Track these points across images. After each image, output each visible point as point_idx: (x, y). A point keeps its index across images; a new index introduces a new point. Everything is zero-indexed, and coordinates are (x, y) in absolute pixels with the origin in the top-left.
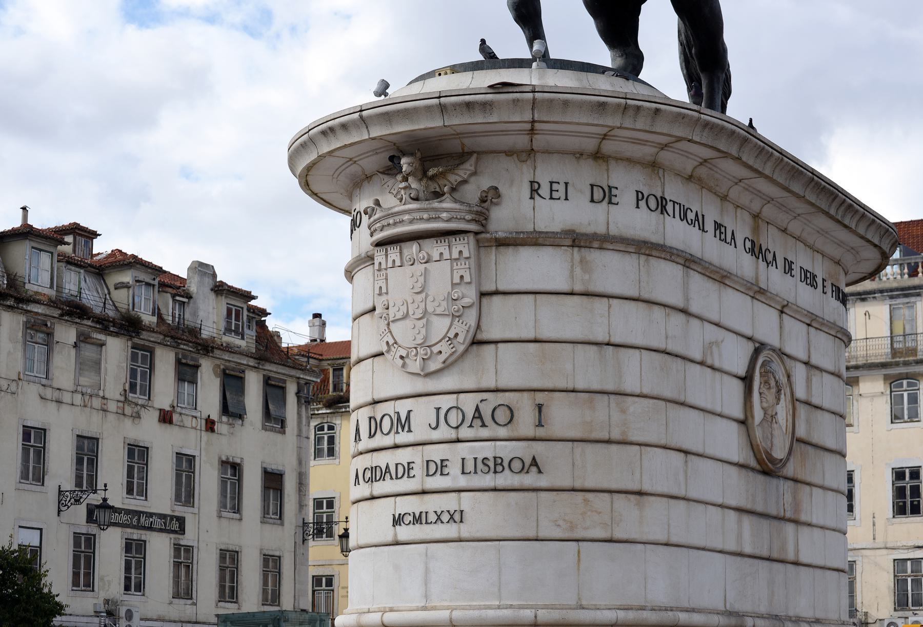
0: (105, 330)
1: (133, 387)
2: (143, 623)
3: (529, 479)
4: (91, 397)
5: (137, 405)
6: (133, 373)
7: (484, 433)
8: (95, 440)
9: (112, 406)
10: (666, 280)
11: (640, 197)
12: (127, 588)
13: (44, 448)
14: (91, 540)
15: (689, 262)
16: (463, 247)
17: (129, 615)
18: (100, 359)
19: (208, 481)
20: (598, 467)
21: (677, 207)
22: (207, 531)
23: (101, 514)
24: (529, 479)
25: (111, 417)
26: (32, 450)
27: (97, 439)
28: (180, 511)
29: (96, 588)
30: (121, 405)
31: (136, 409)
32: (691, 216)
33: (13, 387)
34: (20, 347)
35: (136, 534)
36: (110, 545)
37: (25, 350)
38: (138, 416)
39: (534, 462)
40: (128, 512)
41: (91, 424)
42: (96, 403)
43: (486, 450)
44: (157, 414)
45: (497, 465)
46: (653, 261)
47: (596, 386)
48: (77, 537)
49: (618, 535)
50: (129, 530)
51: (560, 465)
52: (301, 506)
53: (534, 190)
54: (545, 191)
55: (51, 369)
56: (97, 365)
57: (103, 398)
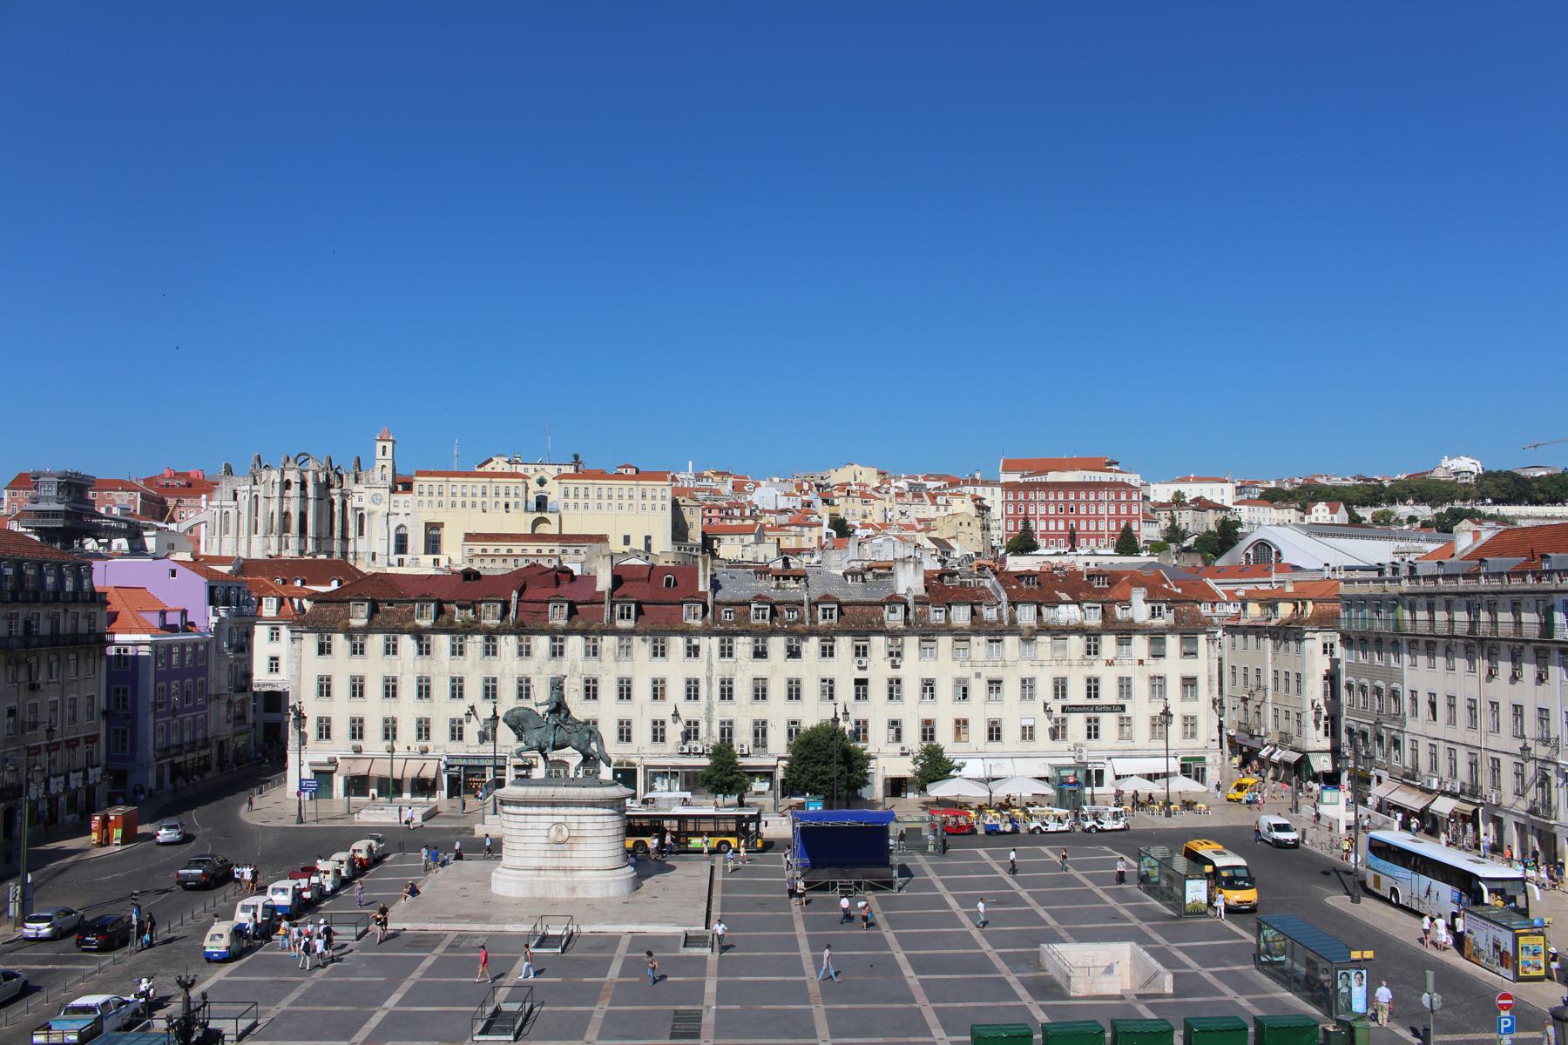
1: (1089, 653)
8: (1064, 680)
10: (521, 818)
12: (1089, 736)
19: (1141, 687)
22: (1142, 708)
28: (1121, 702)
36: (1077, 723)
52: (1210, 691)
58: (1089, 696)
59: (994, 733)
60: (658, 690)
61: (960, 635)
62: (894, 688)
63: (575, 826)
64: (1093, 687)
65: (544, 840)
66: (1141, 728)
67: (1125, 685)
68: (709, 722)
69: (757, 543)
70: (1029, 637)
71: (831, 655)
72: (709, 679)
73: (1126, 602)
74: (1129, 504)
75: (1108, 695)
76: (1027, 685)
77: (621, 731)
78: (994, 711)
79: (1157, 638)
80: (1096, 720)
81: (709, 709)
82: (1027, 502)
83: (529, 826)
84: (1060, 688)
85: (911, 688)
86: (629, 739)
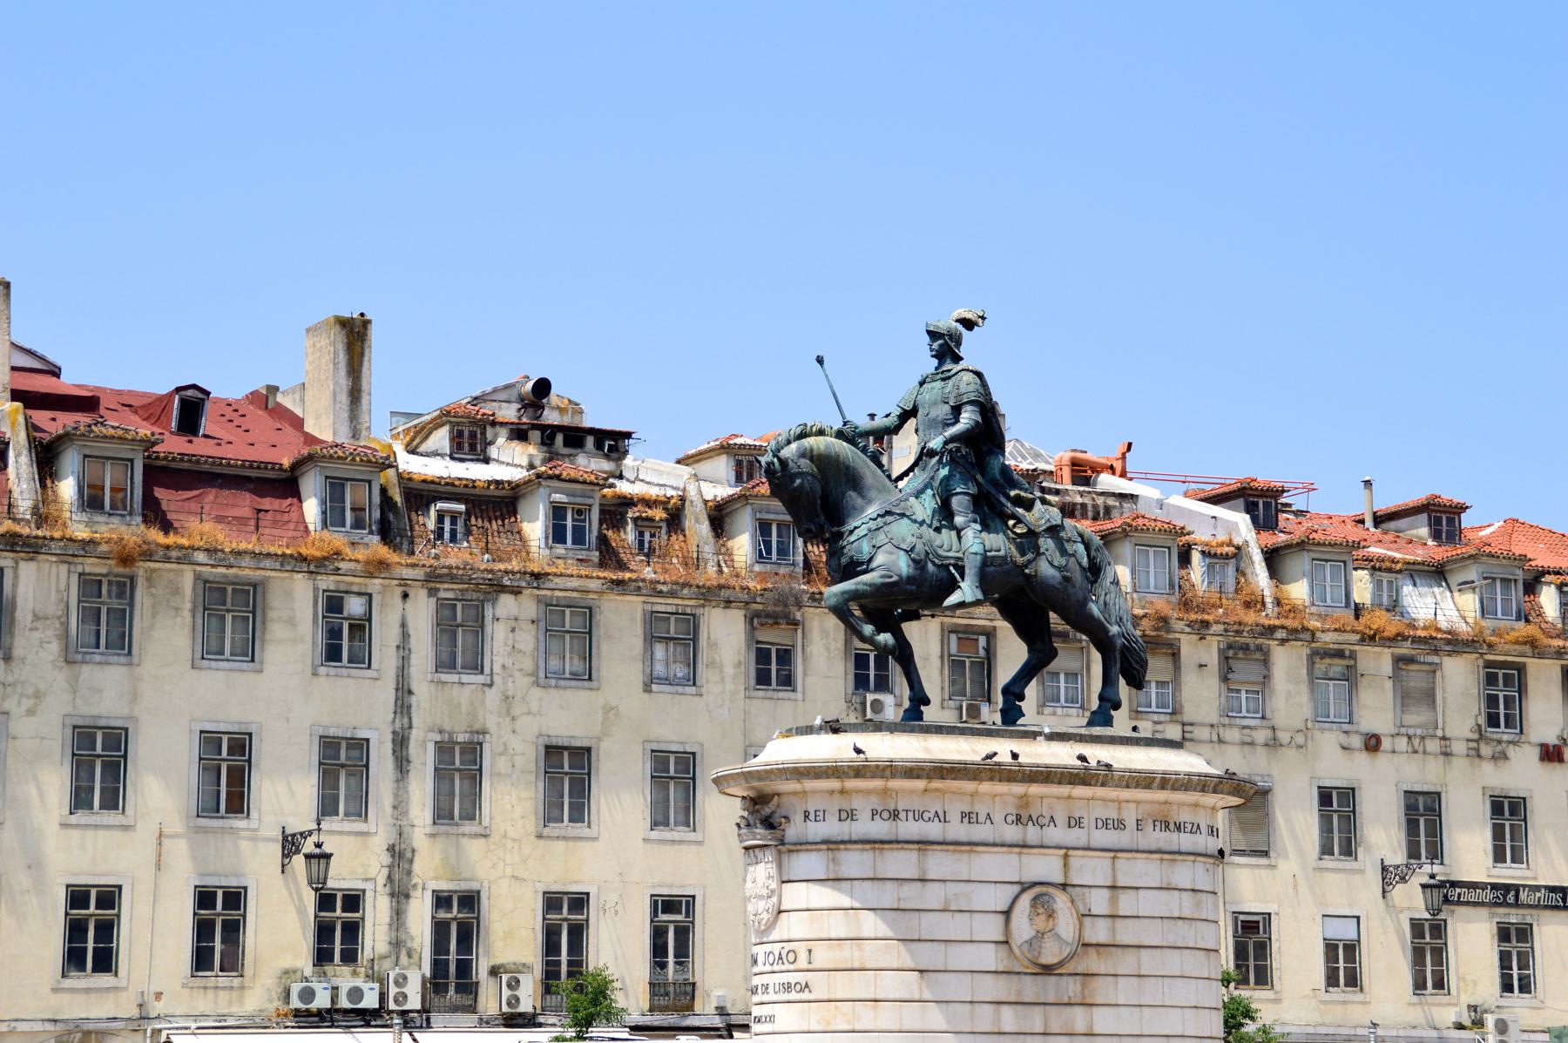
0: (1436, 651)
1: (1493, 721)
2: (1526, 1036)
3: (805, 996)
4: (1428, 740)
5: (1499, 742)
6: (1492, 701)
7: (784, 968)
9: (1459, 748)
11: (874, 813)
12: (1507, 987)
13: (1354, 812)
14: (1439, 930)
15: (923, 844)
16: (769, 855)
17: (1502, 1027)
18: (1434, 689)
20: (843, 985)
21: (911, 815)
23: (1446, 893)
24: (805, 996)
25: (1459, 764)
26: (1335, 817)
27: (1439, 794)
29: (1453, 991)
30: (1474, 745)
31: (1499, 748)
32: (926, 816)
33: (1300, 739)
34: (1304, 689)
35: (1514, 917)
37: (1312, 691)
38: (1504, 756)
39: (807, 986)
40: (1495, 887)
41: (1422, 774)
42: (1433, 746)
43: (785, 978)
44: (1536, 752)
45: (788, 987)
46: (887, 854)
47: (843, 935)
48: (1417, 927)
49: (857, 1028)
50: (1501, 910)
51: (821, 986)
53: (806, 817)
54: (812, 817)
55: (1355, 709)
56: (1429, 697)
57: (1444, 738)
58: (1499, 857)
63: (1099, 902)
65: (989, 958)
68: (400, 895)
69: (276, 389)
71: (787, 681)
72: (400, 742)
76: (1338, 809)
77: (75, 930)
80: (1525, 933)
81: (400, 856)
83: (933, 896)
84: (1423, 816)
86: (105, 962)
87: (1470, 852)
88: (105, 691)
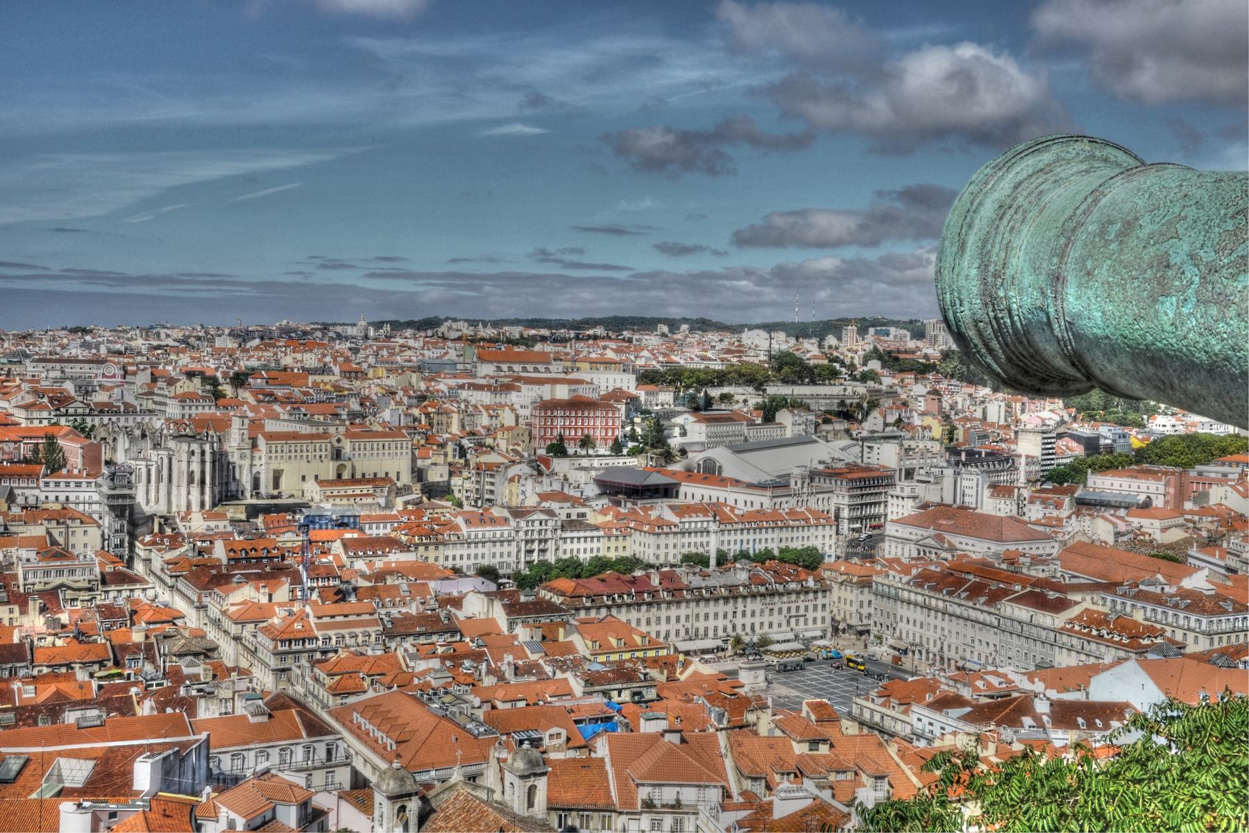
19: (811, 608)
22: (810, 615)
59: (771, 625)
60: (678, 620)
61: (763, 595)
62: (744, 614)
64: (798, 608)
66: (810, 622)
67: (806, 608)
70: (781, 595)
73: (806, 581)
74: (614, 419)
75: (802, 612)
76: (780, 610)
78: (771, 619)
79: (816, 592)
82: (552, 418)
84: (789, 609)
85: (748, 613)
87: (793, 613)
88: (669, 613)
